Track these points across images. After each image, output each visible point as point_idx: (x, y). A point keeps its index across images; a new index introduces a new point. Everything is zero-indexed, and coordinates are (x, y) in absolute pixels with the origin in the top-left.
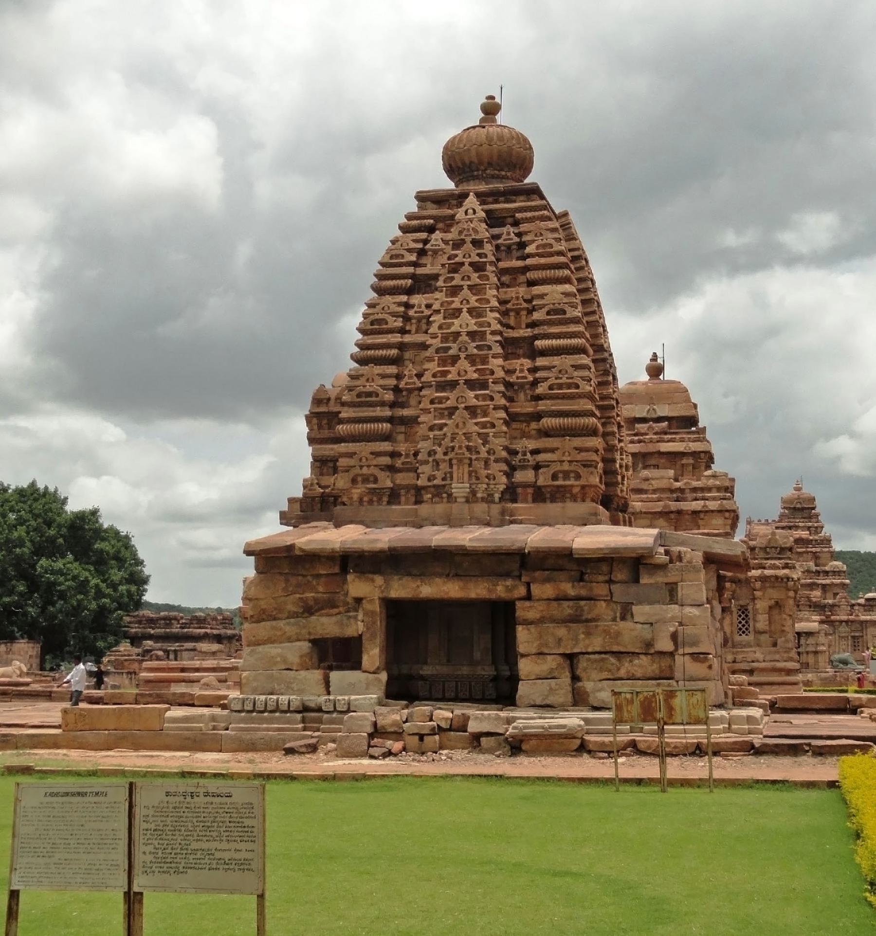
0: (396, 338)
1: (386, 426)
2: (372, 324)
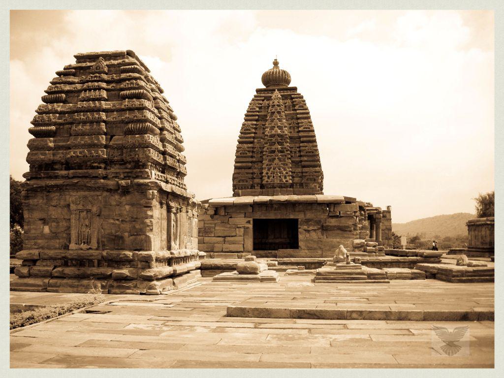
0: (253, 135)
1: (250, 164)
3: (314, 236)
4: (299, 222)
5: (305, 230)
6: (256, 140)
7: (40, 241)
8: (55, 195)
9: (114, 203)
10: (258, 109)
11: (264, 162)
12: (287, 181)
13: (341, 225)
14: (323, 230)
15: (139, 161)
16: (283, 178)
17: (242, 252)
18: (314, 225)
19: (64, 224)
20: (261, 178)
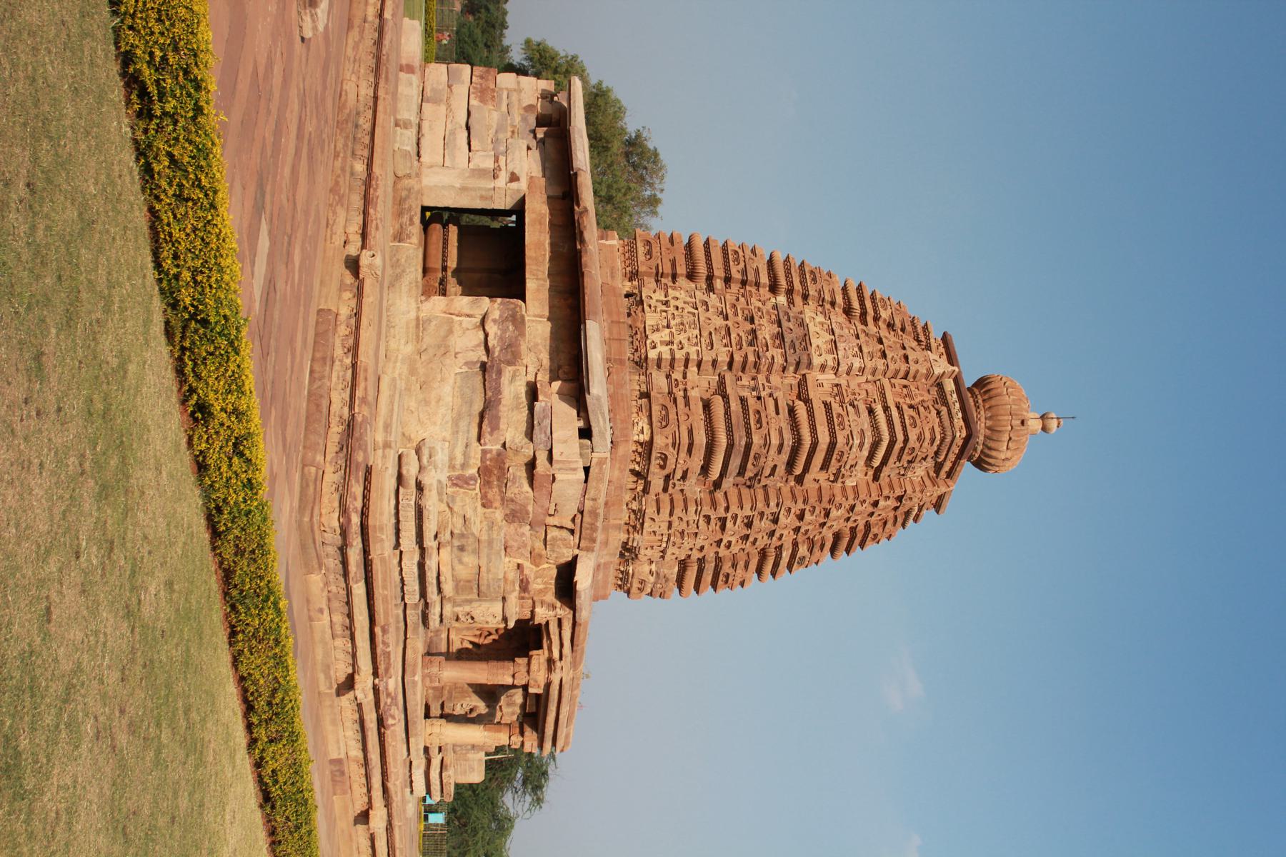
2: (812, 272)
3: (467, 343)
6: (782, 299)
13: (501, 408)
16: (665, 335)
18: (501, 338)
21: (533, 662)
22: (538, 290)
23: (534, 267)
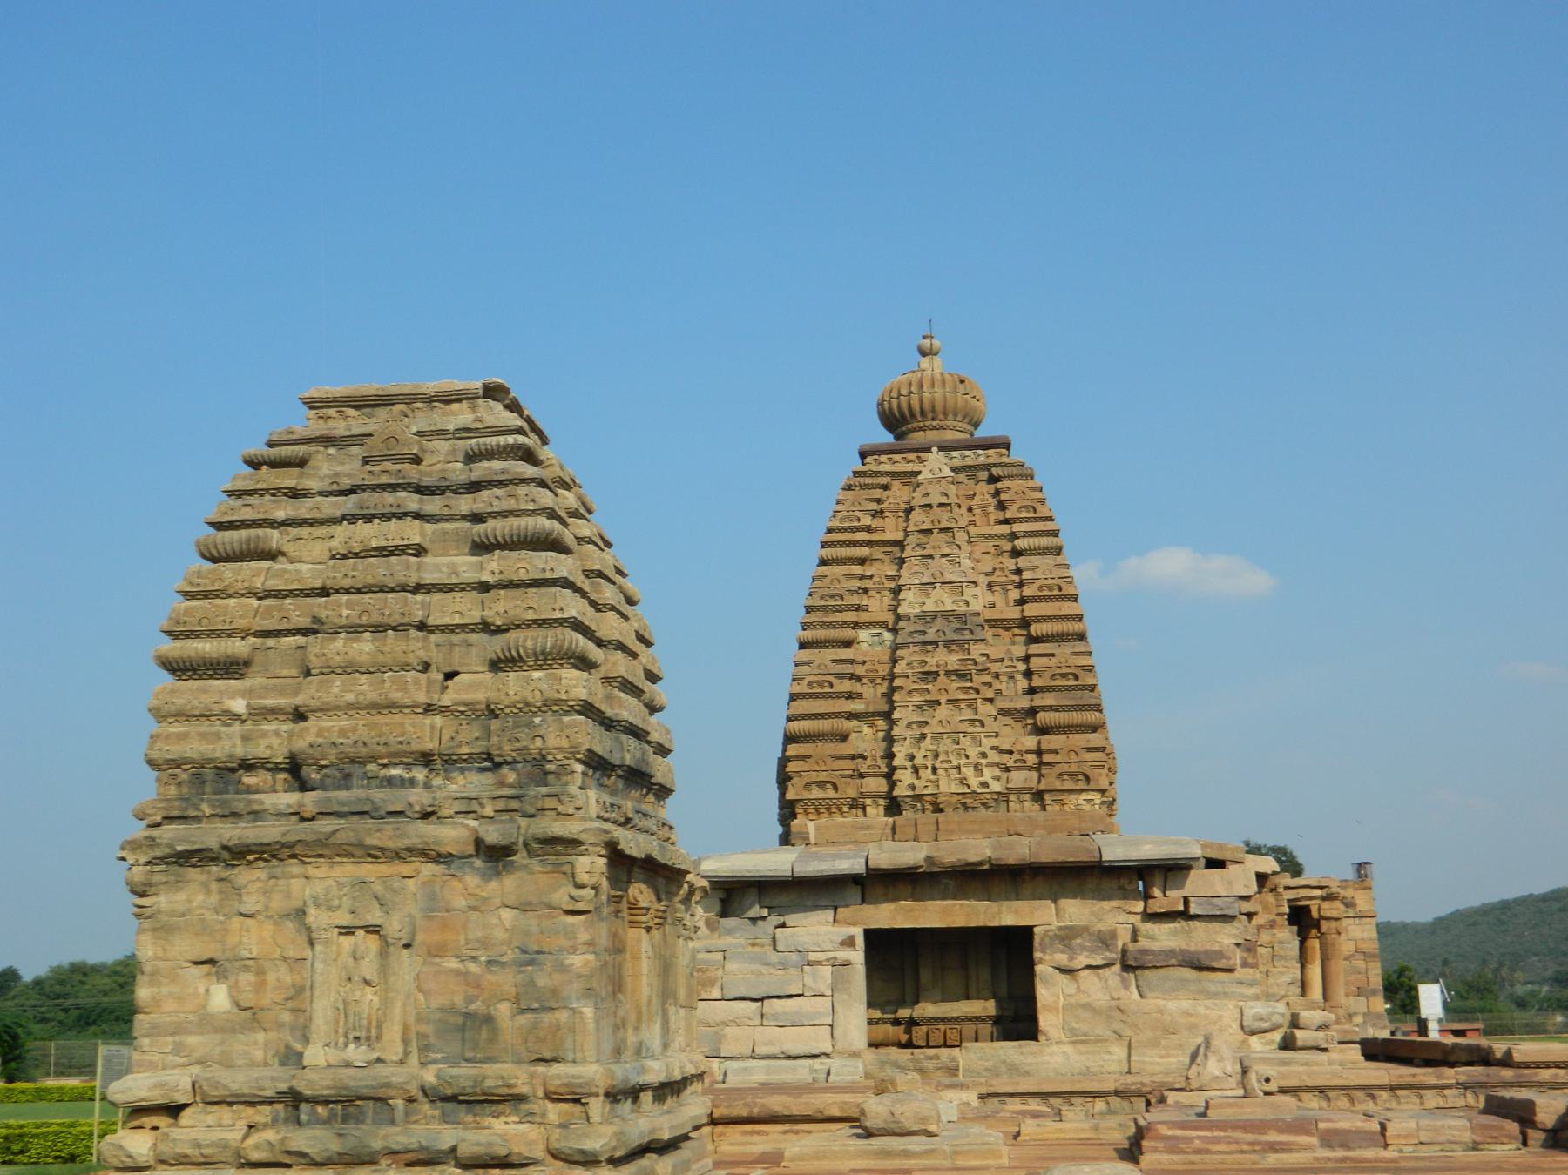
4: (1037, 940)
5: (1063, 971)
7: (192, 1040)
8: (250, 877)
9: (460, 902)
10: (867, 520)
11: (896, 715)
12: (985, 785)
13: (1192, 948)
14: (1126, 968)
15: (544, 757)
16: (969, 772)
17: (827, 1055)
19: (280, 976)
20: (889, 776)
21: (1328, 914)
22: (1017, 912)
23: (982, 916)
